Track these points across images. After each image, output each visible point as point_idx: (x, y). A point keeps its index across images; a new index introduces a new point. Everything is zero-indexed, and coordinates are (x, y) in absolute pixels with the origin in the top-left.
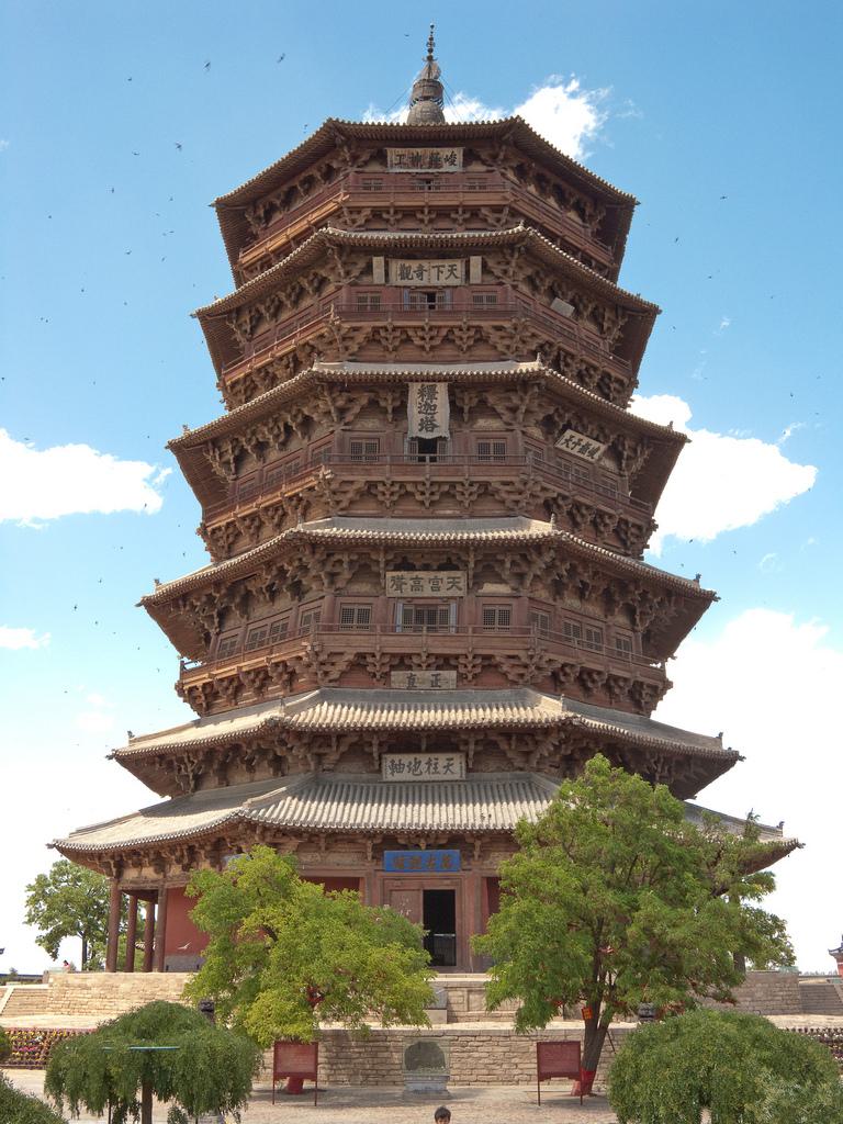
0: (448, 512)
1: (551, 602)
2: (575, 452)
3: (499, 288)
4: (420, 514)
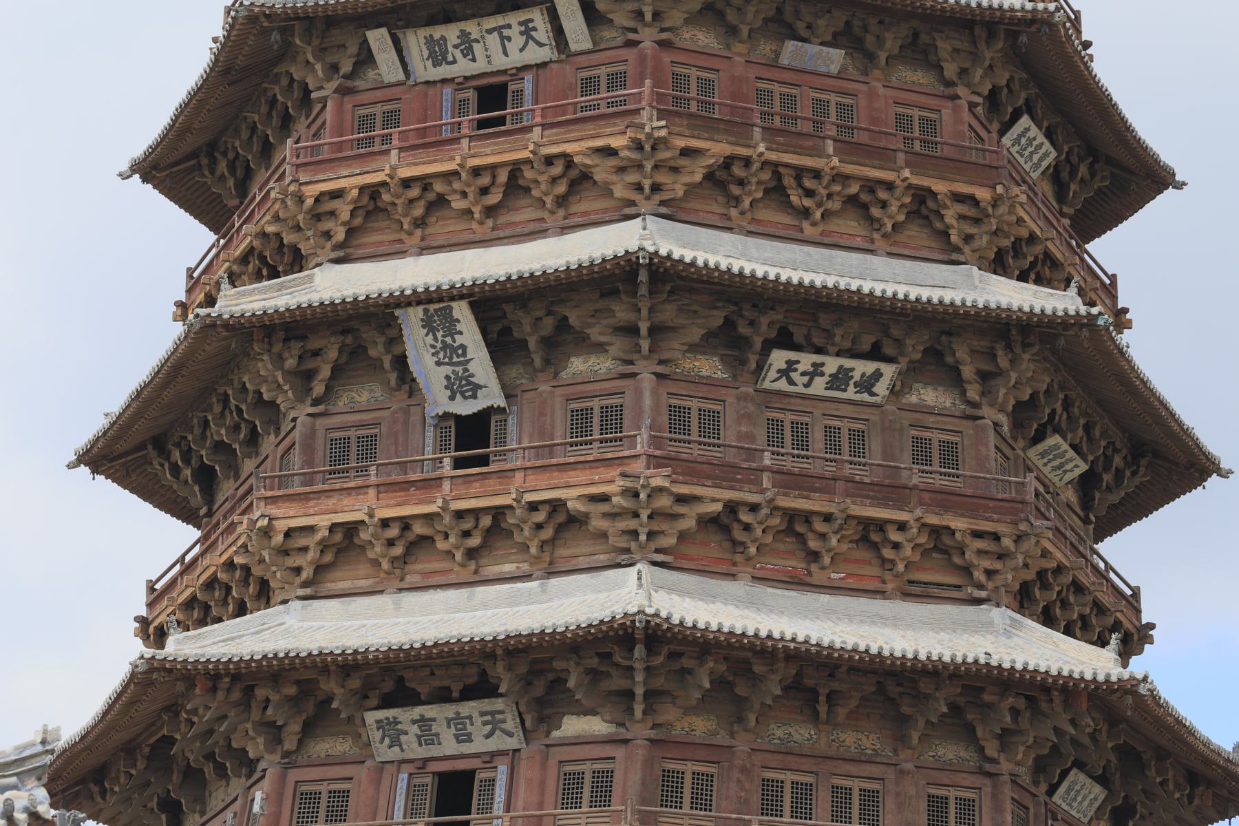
0: (508, 568)
1: (722, 739)
3: (630, 54)
4: (452, 578)
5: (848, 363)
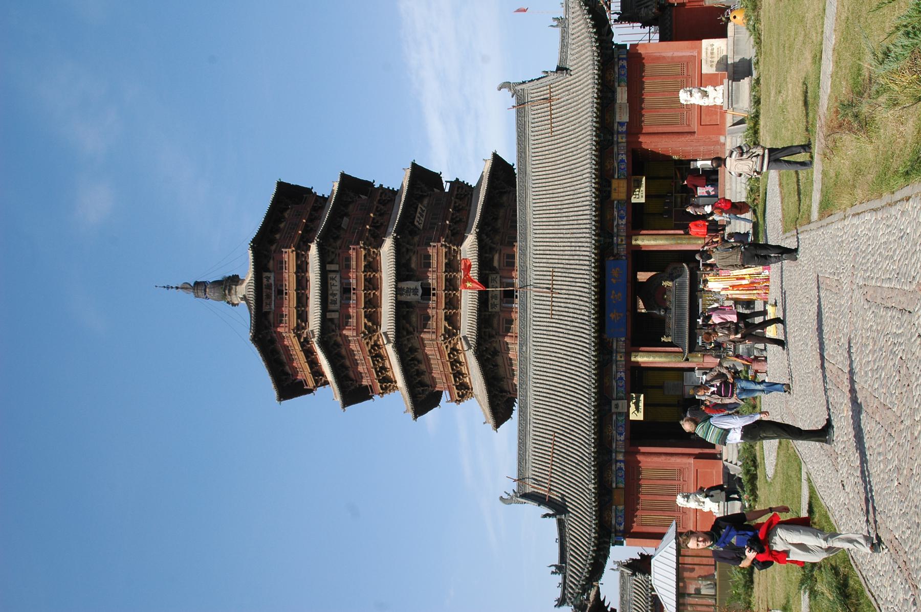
2: (423, 219)
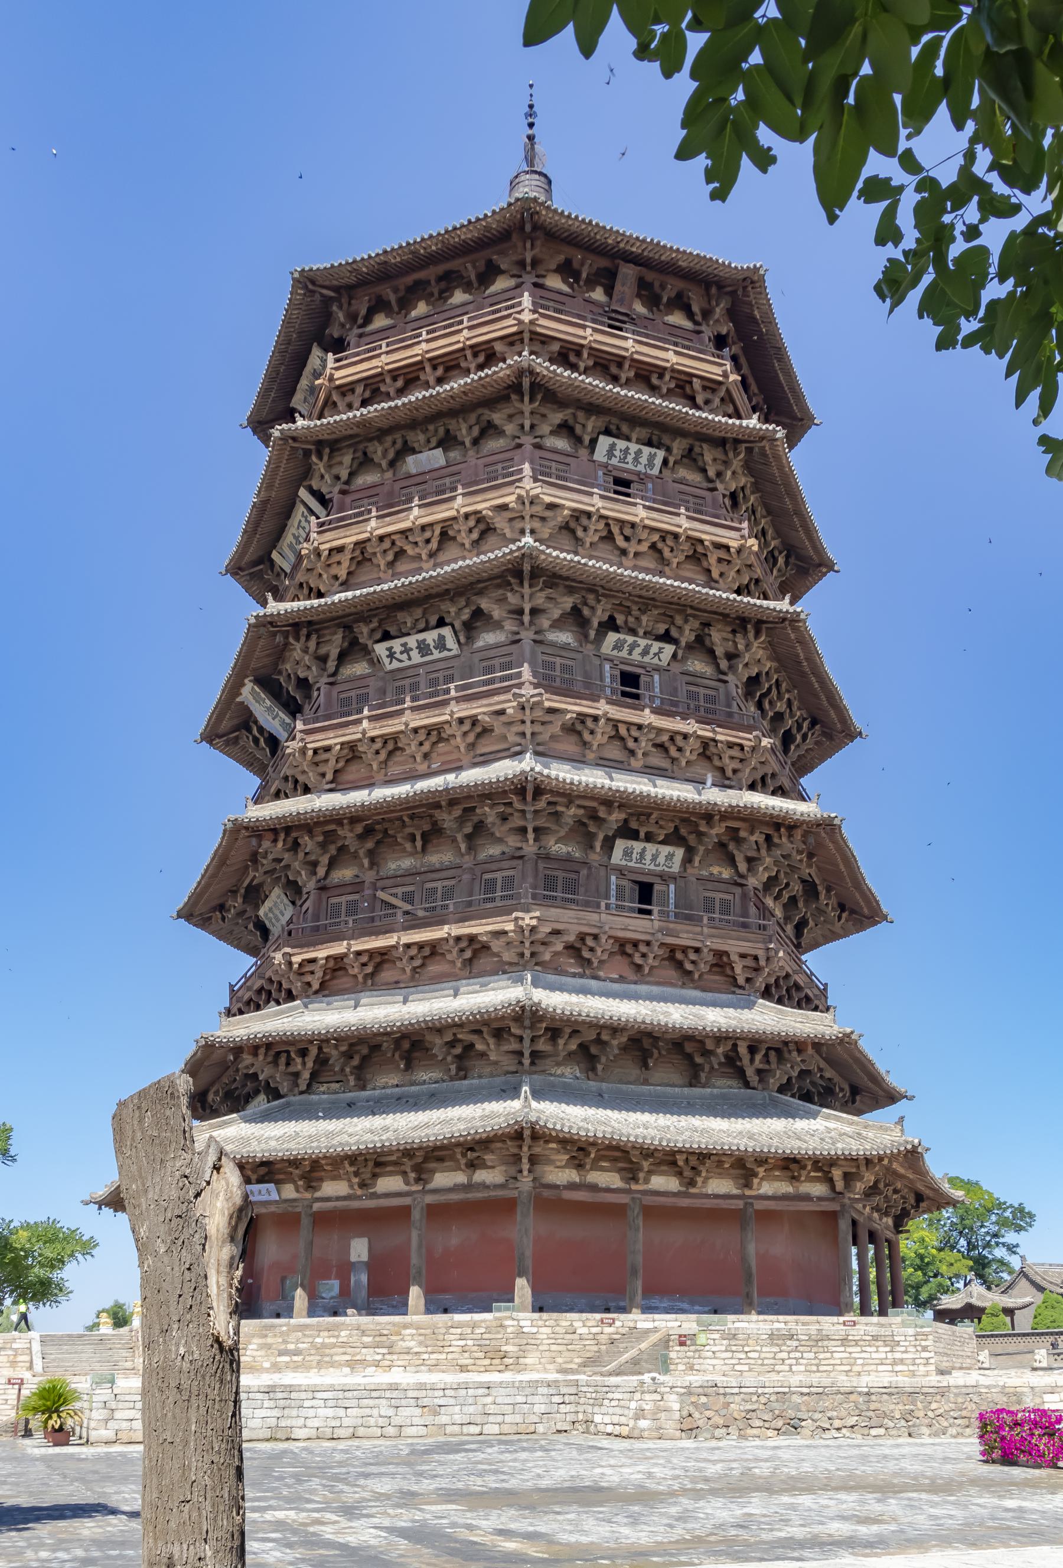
5: (421, 636)
